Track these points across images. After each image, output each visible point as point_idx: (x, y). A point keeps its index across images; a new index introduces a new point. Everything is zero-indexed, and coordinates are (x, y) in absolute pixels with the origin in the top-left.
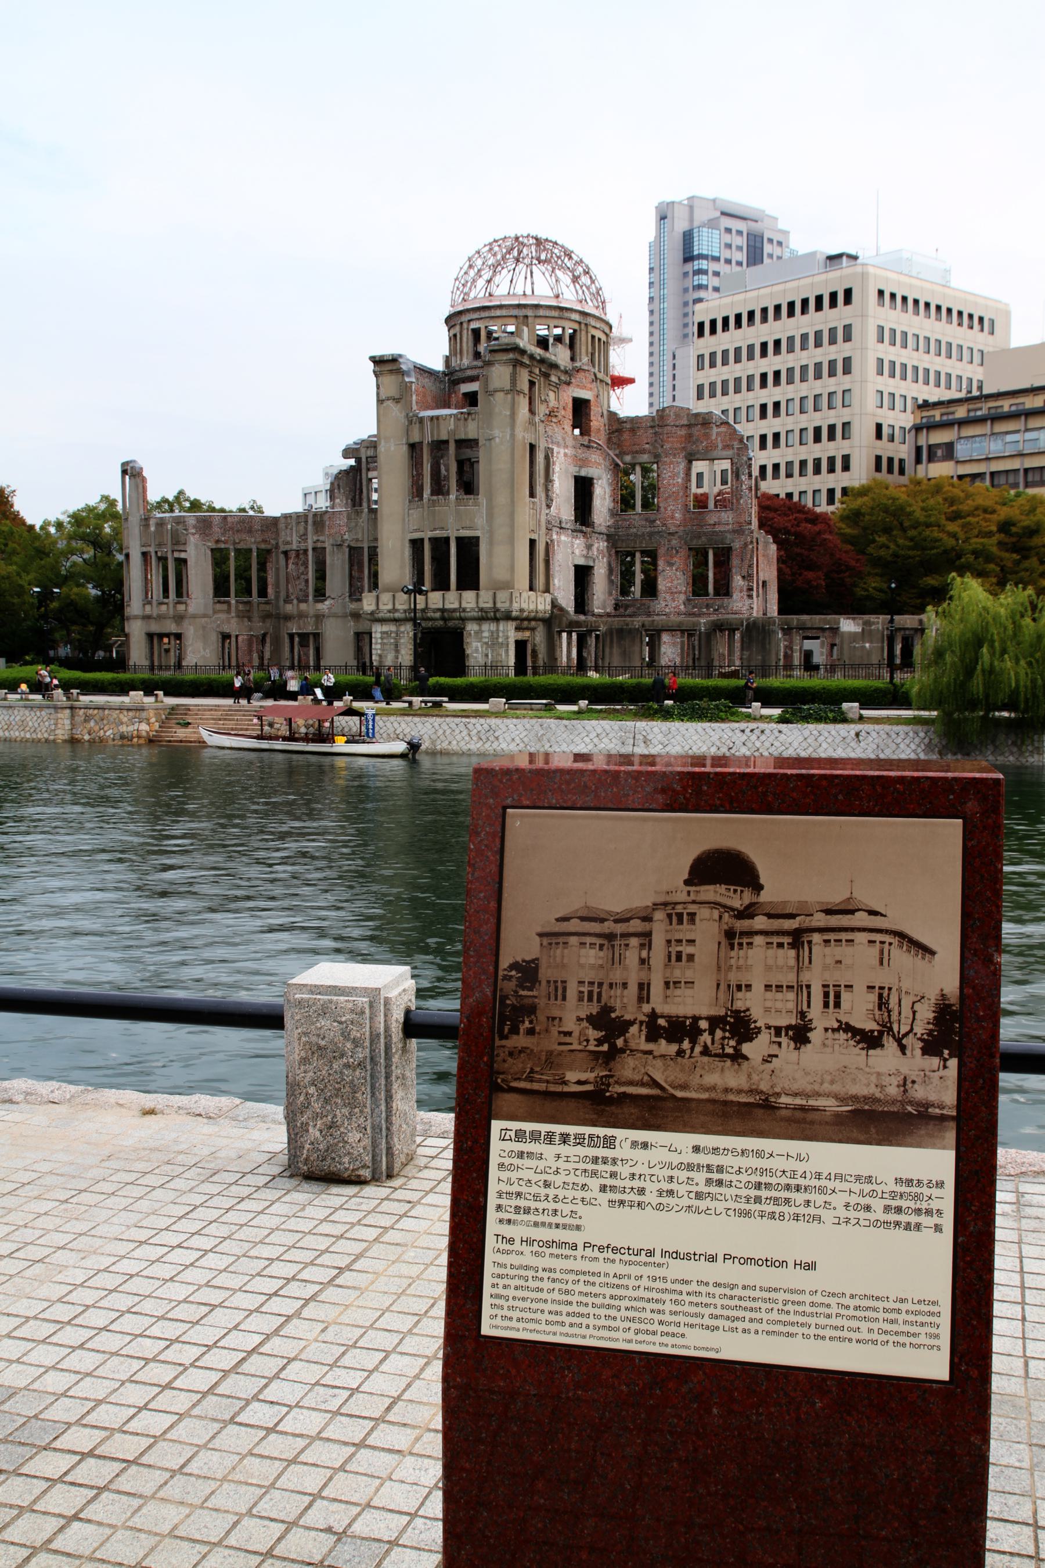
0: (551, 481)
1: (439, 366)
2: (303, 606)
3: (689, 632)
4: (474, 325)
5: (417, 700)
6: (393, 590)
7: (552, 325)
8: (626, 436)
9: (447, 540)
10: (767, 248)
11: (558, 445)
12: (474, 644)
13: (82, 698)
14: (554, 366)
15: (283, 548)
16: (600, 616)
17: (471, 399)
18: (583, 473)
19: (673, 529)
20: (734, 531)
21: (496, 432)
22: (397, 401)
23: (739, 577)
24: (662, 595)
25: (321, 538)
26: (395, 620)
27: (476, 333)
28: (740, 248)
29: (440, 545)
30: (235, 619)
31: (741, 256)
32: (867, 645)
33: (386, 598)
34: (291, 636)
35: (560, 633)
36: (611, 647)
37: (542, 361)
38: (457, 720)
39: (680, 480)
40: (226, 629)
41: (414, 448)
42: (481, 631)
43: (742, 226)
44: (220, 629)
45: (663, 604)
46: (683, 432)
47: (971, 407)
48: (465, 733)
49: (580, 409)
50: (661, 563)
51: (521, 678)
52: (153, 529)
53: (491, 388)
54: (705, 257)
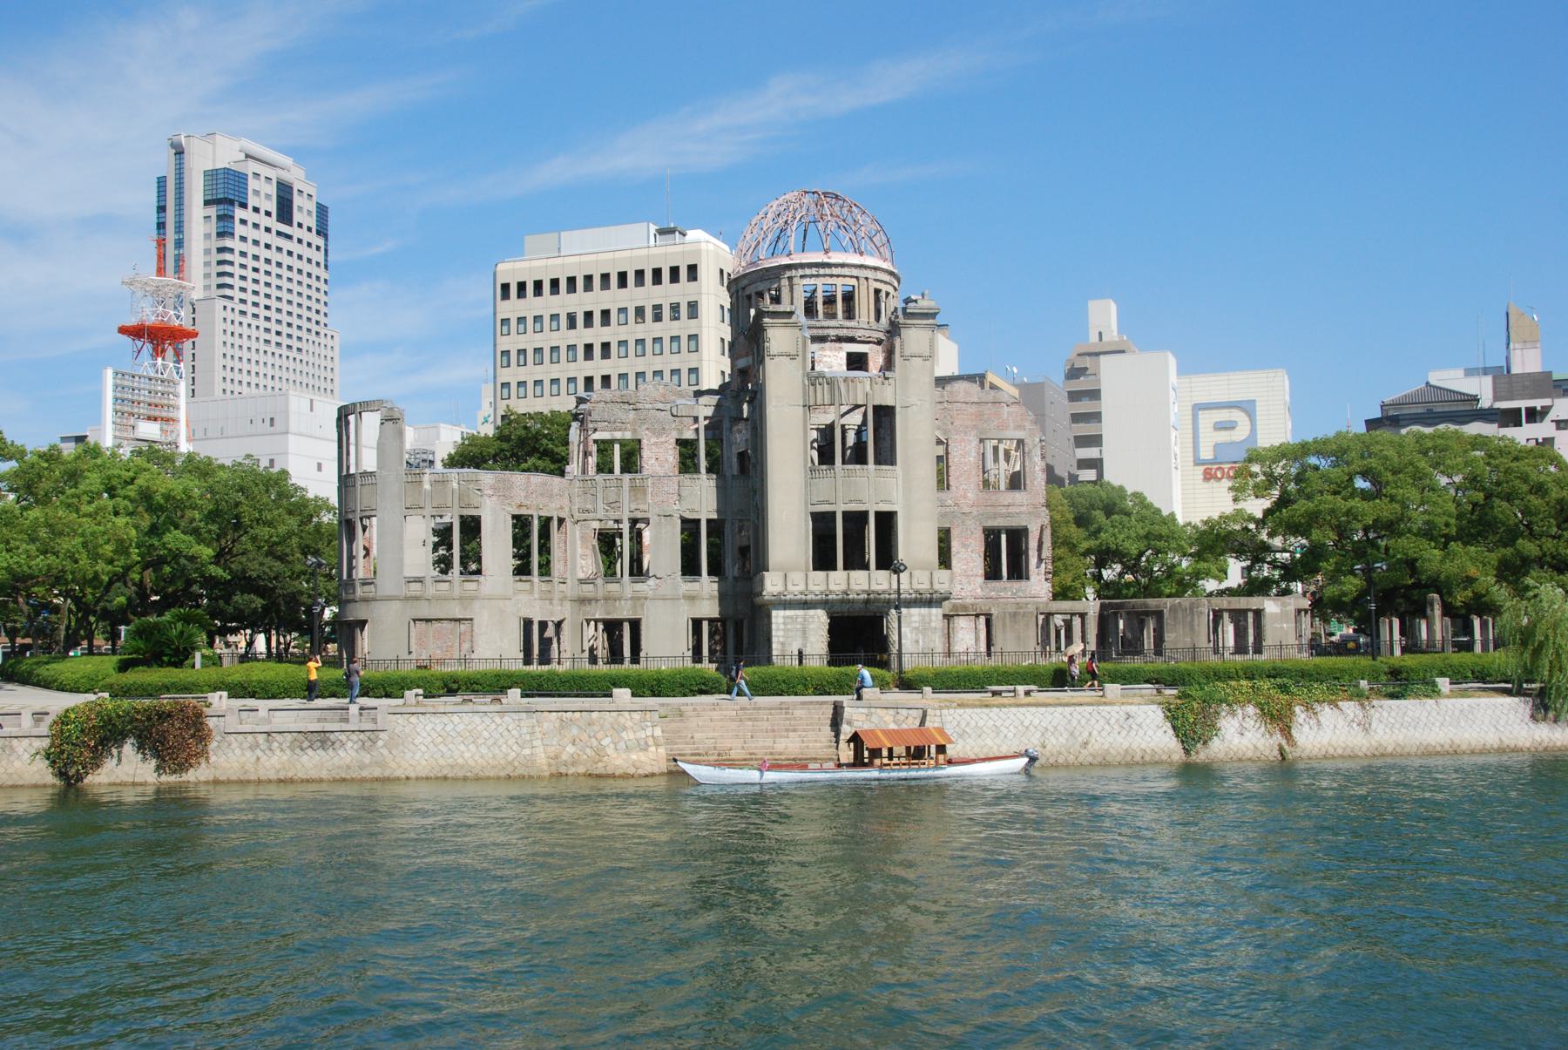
2: (613, 587)
9: (865, 514)
10: (297, 201)
19: (966, 510)
22: (792, 357)
25: (642, 507)
28: (268, 196)
29: (856, 520)
31: (272, 206)
39: (972, 459)
45: (960, 587)
46: (973, 409)
48: (1102, 722)
50: (955, 545)
52: (427, 486)
54: (231, 202)
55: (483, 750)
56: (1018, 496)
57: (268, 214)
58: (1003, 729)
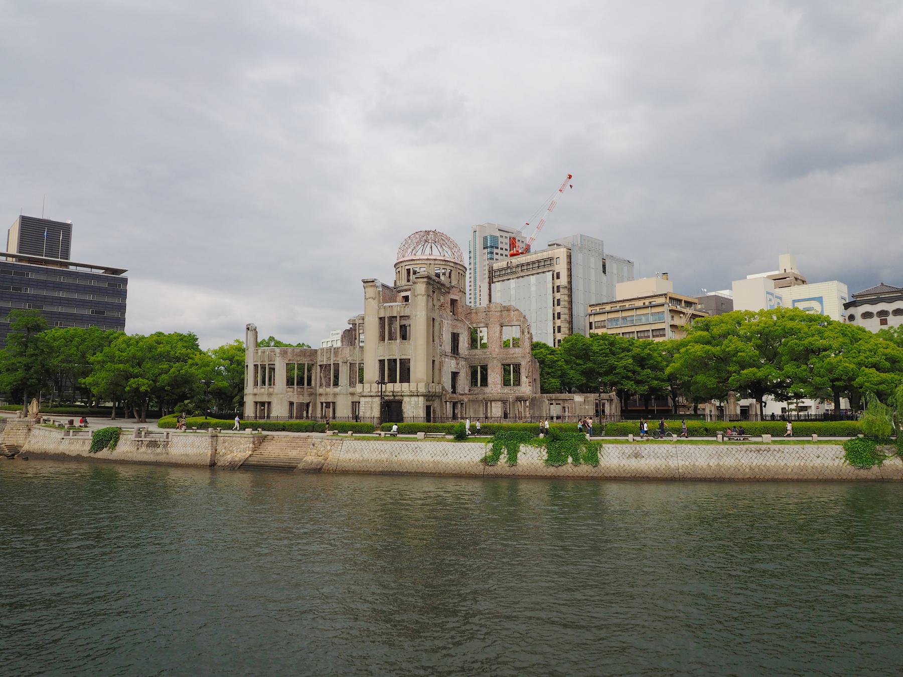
0: (442, 335)
1: (392, 285)
2: (328, 390)
3: (504, 402)
4: (407, 267)
5: (383, 433)
6: (371, 383)
7: (441, 268)
8: (473, 315)
9: (395, 360)
11: (445, 319)
12: (408, 407)
13: (222, 431)
14: (443, 285)
15: (319, 363)
16: (462, 395)
17: (406, 299)
21: (418, 313)
22: (374, 299)
23: (525, 377)
24: (490, 386)
25: (338, 359)
26: (371, 396)
27: (408, 270)
28: (506, 244)
33: (367, 386)
34: (322, 403)
35: (446, 402)
36: (470, 409)
37: (438, 282)
38: (402, 442)
40: (292, 400)
41: (382, 319)
42: (411, 401)
43: (508, 235)
44: (289, 400)
46: (499, 314)
47: (612, 306)
49: (453, 302)
50: (489, 371)
51: (429, 424)
52: (260, 354)
53: (416, 294)
55: (195, 449)
56: (517, 350)
57: (506, 250)
58: (365, 450)
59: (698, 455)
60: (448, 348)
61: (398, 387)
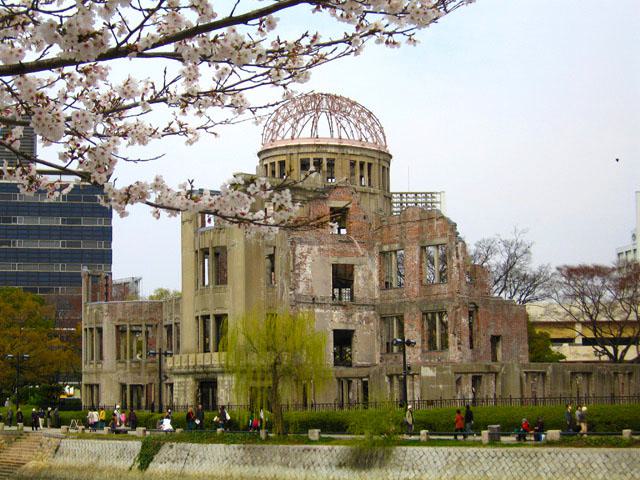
6: (188, 352)
8: (385, 231)
11: (310, 243)
15: (165, 323)
18: (342, 261)
20: (449, 299)
21: (236, 241)
29: (206, 318)
30: (129, 374)
32: (441, 386)
40: (123, 380)
42: (223, 381)
50: (406, 325)
59: (432, 462)
60: (324, 288)
61: (214, 359)
